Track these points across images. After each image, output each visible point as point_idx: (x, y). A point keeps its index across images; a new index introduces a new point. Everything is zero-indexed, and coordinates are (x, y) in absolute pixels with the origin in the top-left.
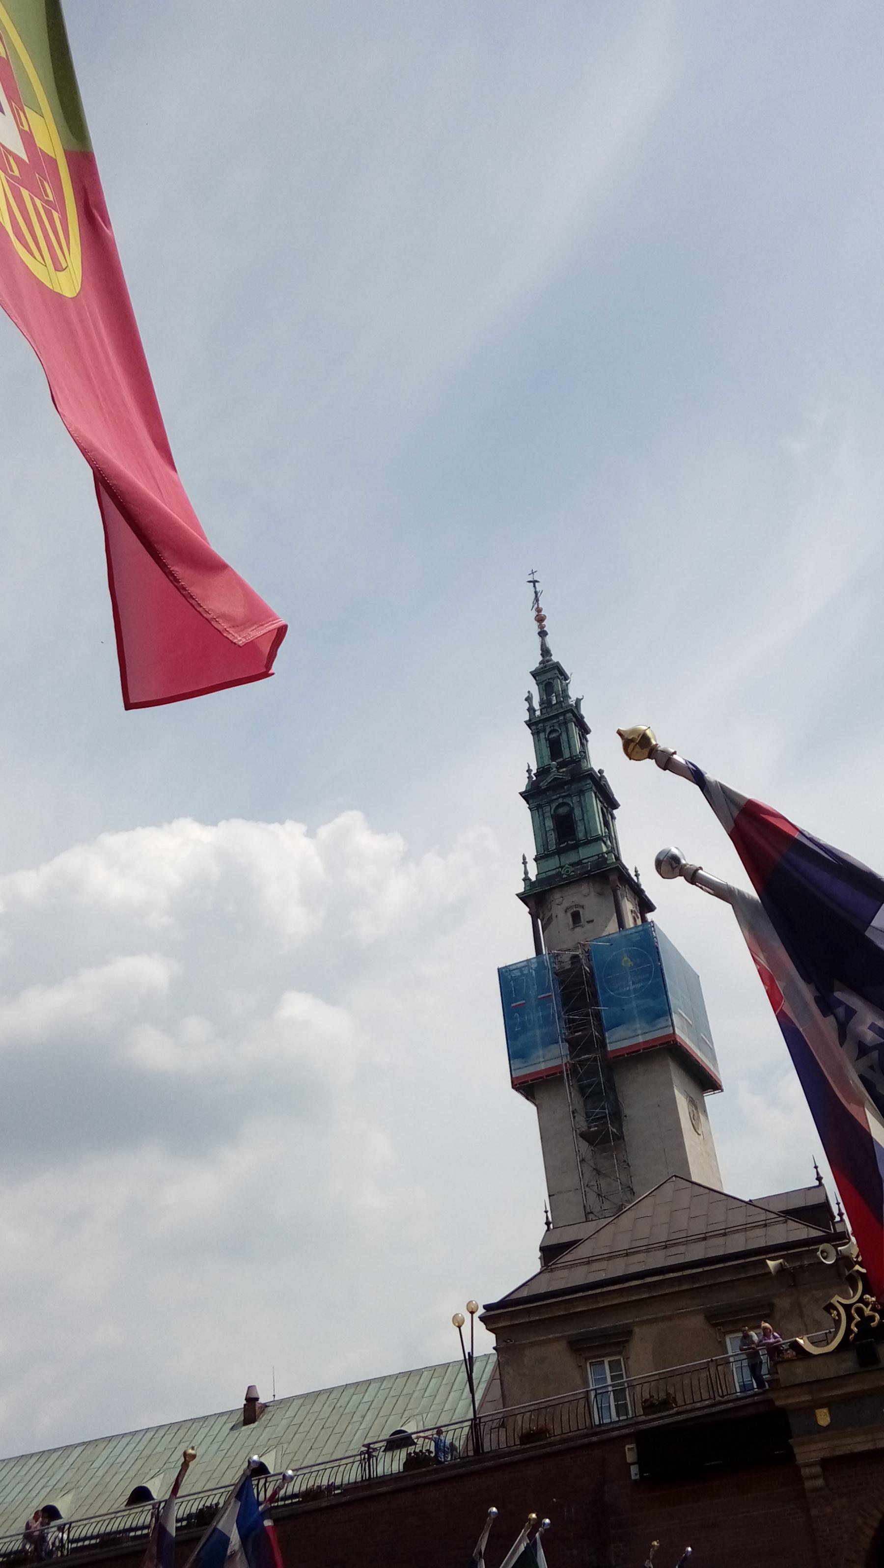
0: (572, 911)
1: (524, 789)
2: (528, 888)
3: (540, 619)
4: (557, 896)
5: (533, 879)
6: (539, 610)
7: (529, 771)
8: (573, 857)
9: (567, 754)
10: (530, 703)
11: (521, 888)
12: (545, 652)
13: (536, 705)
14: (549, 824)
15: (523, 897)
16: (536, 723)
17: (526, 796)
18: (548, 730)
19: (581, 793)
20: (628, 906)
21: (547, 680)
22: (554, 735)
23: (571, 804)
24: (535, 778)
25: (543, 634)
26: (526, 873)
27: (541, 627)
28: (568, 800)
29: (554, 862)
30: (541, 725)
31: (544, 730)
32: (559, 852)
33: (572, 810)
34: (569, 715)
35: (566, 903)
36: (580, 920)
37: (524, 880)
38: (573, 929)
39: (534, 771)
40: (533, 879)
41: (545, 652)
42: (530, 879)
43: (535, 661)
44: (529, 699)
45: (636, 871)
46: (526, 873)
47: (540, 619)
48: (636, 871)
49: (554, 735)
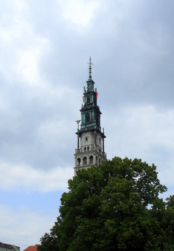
1: (80, 109)
3: (90, 69)
4: (83, 135)
5: (80, 130)
6: (90, 67)
7: (82, 105)
8: (88, 126)
9: (91, 102)
10: (85, 89)
11: (77, 131)
12: (90, 77)
13: (86, 90)
14: (84, 118)
15: (77, 134)
17: (81, 111)
18: (88, 96)
19: (92, 112)
20: (99, 137)
25: (90, 72)
26: (78, 128)
27: (90, 71)
29: (83, 127)
32: (86, 124)
33: (90, 115)
34: (92, 93)
35: (85, 136)
37: (78, 130)
38: (85, 142)
39: (83, 105)
41: (90, 77)
43: (87, 79)
44: (84, 88)
45: (103, 128)
46: (78, 128)
47: (90, 69)
48: (103, 128)
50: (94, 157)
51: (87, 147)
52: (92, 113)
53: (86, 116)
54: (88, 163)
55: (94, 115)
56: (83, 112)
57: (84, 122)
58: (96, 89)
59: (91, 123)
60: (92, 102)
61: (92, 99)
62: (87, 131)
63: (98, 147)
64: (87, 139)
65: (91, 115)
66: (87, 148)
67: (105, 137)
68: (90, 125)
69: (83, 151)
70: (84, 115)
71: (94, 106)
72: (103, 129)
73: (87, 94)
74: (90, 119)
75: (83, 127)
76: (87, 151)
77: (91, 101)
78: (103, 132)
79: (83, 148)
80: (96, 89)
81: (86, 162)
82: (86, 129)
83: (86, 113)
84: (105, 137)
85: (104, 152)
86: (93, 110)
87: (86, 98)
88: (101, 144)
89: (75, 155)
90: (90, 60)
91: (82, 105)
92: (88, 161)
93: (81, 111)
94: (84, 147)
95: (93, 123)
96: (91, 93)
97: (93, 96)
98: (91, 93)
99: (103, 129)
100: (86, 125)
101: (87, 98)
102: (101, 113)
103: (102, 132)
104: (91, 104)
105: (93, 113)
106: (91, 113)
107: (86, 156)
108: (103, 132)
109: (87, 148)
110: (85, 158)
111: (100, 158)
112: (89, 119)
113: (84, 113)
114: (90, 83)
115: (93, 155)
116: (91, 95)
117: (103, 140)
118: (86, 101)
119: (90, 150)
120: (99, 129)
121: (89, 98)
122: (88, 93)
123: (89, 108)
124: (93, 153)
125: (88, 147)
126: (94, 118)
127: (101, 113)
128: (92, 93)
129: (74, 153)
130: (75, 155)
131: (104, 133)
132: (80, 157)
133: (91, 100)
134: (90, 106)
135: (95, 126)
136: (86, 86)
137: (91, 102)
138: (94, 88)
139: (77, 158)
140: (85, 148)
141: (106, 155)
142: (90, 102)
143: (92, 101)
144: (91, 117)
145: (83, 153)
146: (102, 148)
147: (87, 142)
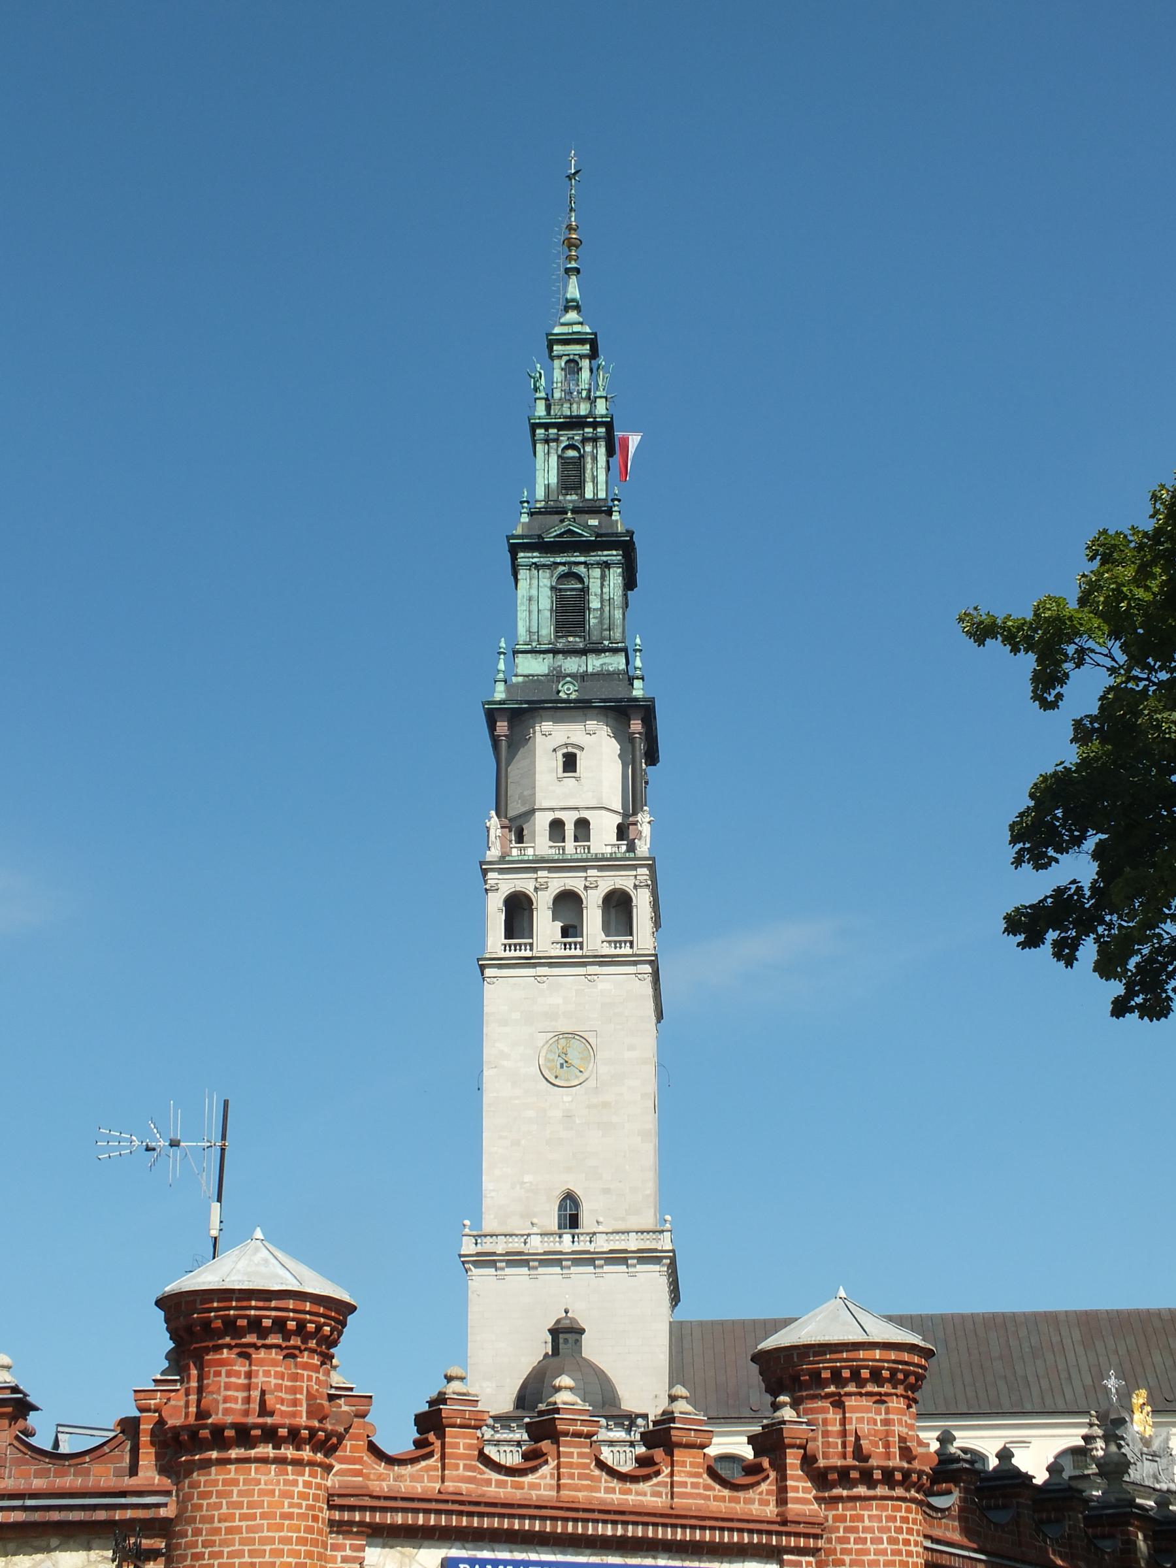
0: (565, 751)
4: (547, 726)
9: (589, 495)
19: (606, 565)
21: (571, 357)
22: (571, 453)
23: (586, 580)
28: (581, 570)
30: (553, 431)
31: (557, 440)
32: (555, 652)
33: (585, 591)
34: (601, 430)
36: (575, 771)
38: (560, 779)
49: (571, 453)
50: (642, 902)
51: (569, 819)
62: (579, 709)
64: (570, 763)
65: (594, 586)
68: (594, 663)
73: (560, 427)
76: (570, 845)
82: (568, 691)
86: (614, 555)
87: (554, 459)
92: (593, 917)
94: (550, 816)
95: (615, 651)
96: (595, 425)
101: (559, 457)
107: (574, 882)
110: (568, 903)
116: (595, 440)
121: (579, 463)
123: (588, 536)
125: (583, 826)
128: (601, 430)
133: (594, 479)
134: (593, 522)
140: (557, 827)
142: (579, 487)
143: (602, 486)
144: (595, 604)
147: (570, 782)
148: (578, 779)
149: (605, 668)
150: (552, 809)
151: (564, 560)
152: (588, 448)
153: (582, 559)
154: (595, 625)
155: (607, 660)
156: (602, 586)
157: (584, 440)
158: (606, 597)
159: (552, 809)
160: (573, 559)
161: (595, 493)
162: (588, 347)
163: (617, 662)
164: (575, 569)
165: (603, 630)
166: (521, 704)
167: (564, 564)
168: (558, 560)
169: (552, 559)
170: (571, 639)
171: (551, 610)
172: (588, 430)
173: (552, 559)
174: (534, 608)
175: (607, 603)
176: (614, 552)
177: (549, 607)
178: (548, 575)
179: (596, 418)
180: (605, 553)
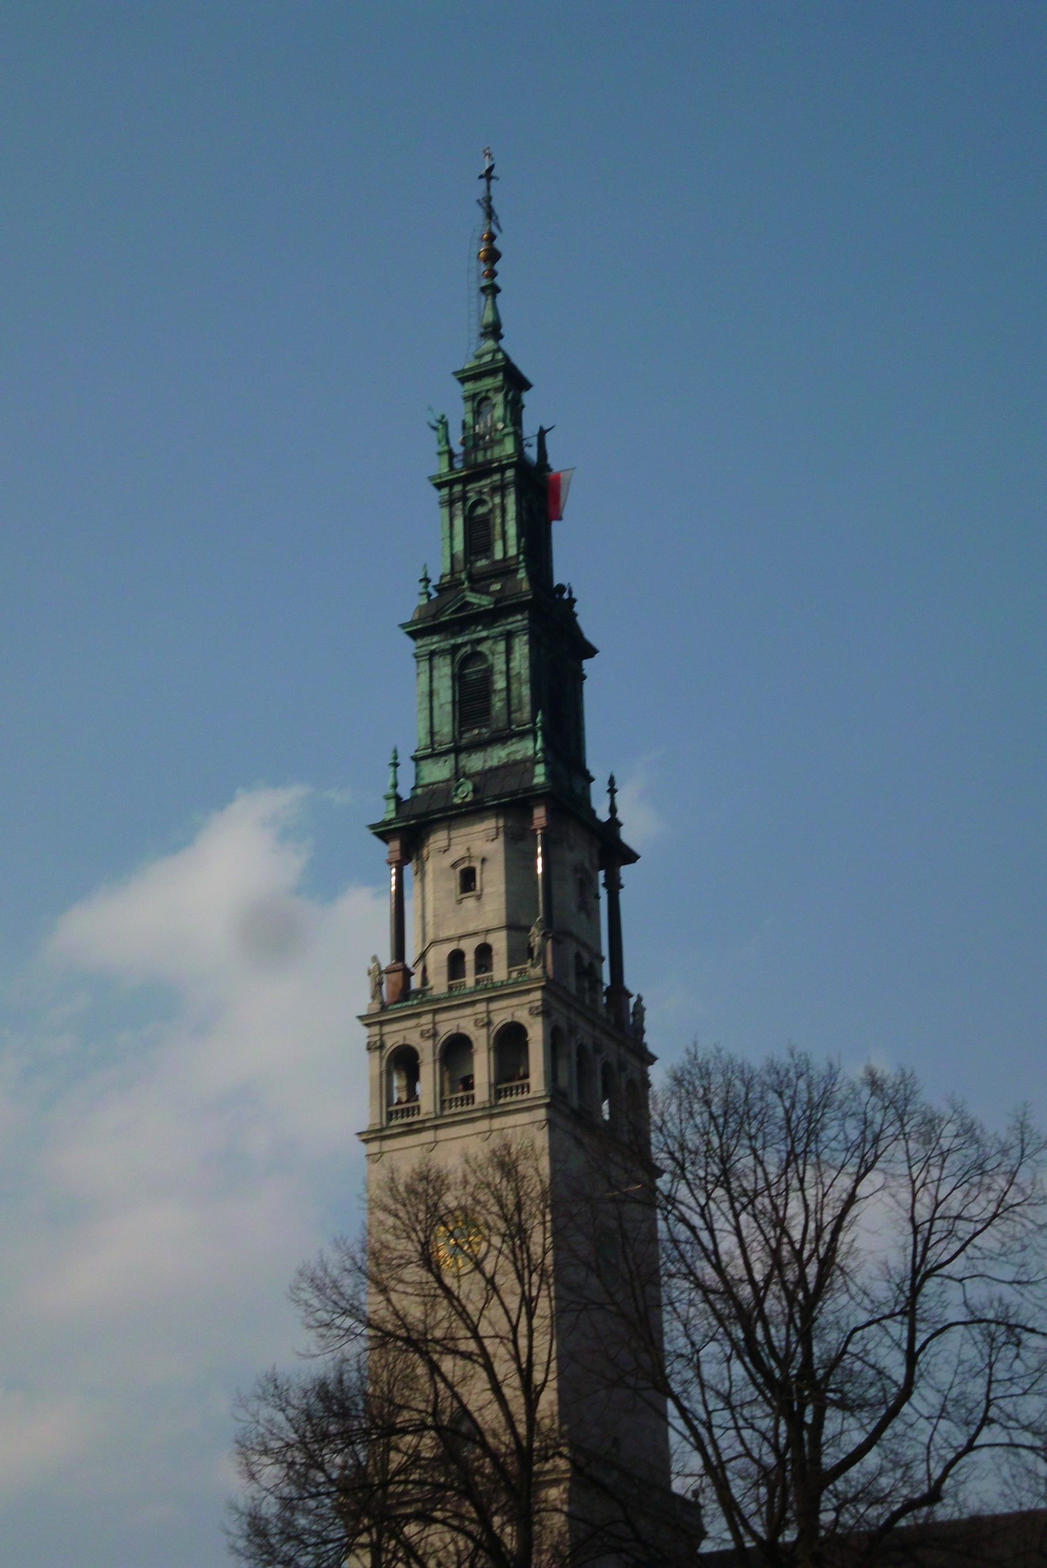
2: (393, 815)
4: (438, 839)
5: (406, 794)
8: (475, 762)
9: (499, 555)
12: (494, 331)
15: (383, 831)
16: (450, 484)
18: (473, 497)
22: (481, 510)
24: (435, 595)
25: (492, 290)
26: (395, 786)
27: (492, 274)
28: (483, 648)
30: (458, 488)
31: (464, 498)
32: (457, 750)
33: (489, 672)
34: (510, 474)
35: (458, 851)
39: (435, 581)
40: (406, 794)
42: (397, 798)
45: (612, 781)
46: (395, 786)
47: (492, 256)
48: (612, 781)
51: (469, 947)
52: (509, 651)
53: (458, 678)
54: (481, 1091)
55: (534, 667)
56: (435, 642)
57: (445, 727)
58: (542, 434)
59: (502, 738)
60: (512, 551)
61: (512, 530)
62: (472, 812)
63: (572, 948)
64: (468, 880)
65: (500, 665)
66: (470, 959)
67: (630, 857)
68: (498, 755)
69: (439, 983)
70: (444, 669)
71: (525, 586)
72: (612, 791)
73: (465, 481)
74: (498, 703)
75: (438, 772)
76: (470, 980)
77: (498, 547)
78: (613, 810)
79: (438, 958)
80: (542, 434)
81: (468, 1083)
83: (456, 648)
84: (630, 857)
85: (618, 991)
86: (518, 621)
87: (459, 523)
88: (593, 914)
89: (367, 1020)
90: (488, 175)
91: (426, 580)
93: (414, 635)
94: (449, 948)
95: (522, 735)
96: (502, 469)
97: (518, 502)
98: (502, 469)
99: (612, 791)
100: (463, 756)
102: (590, 651)
103: (603, 814)
104: (504, 570)
105: (521, 648)
106: (501, 646)
108: (613, 810)
109: (470, 959)
111: (588, 1042)
112: (487, 709)
113: (442, 652)
114: (489, 382)
115: (523, 1016)
116: (500, 489)
117: (614, 886)
118: (459, 546)
119: (500, 971)
120: (578, 790)
122: (478, 472)
124: (526, 999)
125: (484, 952)
126: (526, 691)
127: (590, 651)
128: (510, 474)
129: (364, 1002)
130: (367, 1020)
131: (614, 824)
132: (414, 1039)
134: (496, 587)
135: (533, 761)
136: (459, 413)
137: (499, 555)
138: (530, 430)
139: (392, 1042)
140: (456, 959)
141: (639, 1010)
142: (486, 549)
143: (512, 541)
144: (500, 683)
145: (437, 1000)
146: (605, 951)
147: (470, 903)
148: (479, 898)
149: (512, 757)
150: (449, 940)
151: (466, 638)
152: (497, 500)
153: (484, 634)
154: (501, 708)
155: (512, 748)
156: (508, 661)
157: (494, 490)
158: (513, 673)
159: (449, 940)
160: (475, 636)
161: (505, 552)
162: (500, 377)
163: (527, 748)
164: (479, 648)
165: (509, 713)
166: (409, 820)
167: (464, 644)
168: (460, 640)
169: (452, 642)
170: (476, 732)
171: (454, 703)
172: (497, 477)
173: (452, 642)
174: (436, 704)
175: (513, 680)
176: (519, 617)
177: (450, 699)
178: (448, 660)
179: (502, 460)
180: (511, 620)
